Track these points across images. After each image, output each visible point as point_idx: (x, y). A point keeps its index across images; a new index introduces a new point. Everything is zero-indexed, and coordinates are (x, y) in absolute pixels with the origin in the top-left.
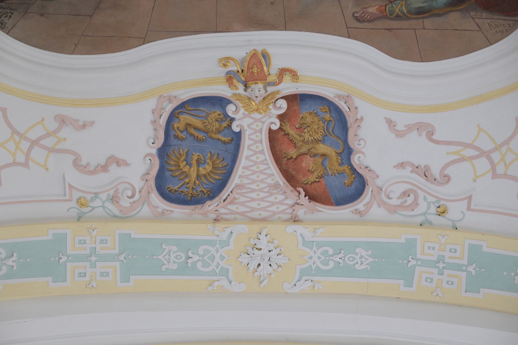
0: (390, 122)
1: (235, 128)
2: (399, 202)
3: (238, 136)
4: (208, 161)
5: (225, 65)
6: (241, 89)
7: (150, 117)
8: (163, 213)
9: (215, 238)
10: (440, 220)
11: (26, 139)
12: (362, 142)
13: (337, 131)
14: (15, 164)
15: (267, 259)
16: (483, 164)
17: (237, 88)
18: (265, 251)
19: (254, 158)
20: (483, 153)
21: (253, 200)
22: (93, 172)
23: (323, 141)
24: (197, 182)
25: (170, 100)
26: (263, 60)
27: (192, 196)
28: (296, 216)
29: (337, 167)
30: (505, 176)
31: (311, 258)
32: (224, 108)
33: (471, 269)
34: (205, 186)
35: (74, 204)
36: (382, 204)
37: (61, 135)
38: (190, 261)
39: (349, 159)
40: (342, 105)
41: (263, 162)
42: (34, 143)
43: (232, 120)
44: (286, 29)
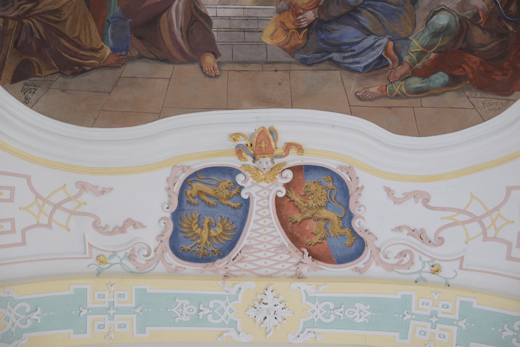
0: (389, 191)
1: (244, 195)
2: (396, 261)
3: (247, 202)
4: (219, 224)
5: (235, 140)
6: (249, 161)
7: (164, 184)
9: (224, 293)
10: (434, 278)
11: (49, 203)
12: (362, 209)
13: (339, 199)
14: (39, 225)
15: (272, 313)
16: (474, 228)
18: (271, 305)
19: (261, 222)
21: (260, 259)
22: (112, 233)
23: (326, 207)
24: (209, 243)
25: (183, 170)
26: (270, 136)
27: (204, 255)
28: (300, 274)
29: (338, 229)
30: (495, 239)
31: (313, 311)
32: (234, 177)
33: (462, 324)
34: (216, 246)
35: (93, 261)
36: (380, 262)
38: (201, 314)
39: (350, 223)
41: (269, 226)
42: (57, 206)
43: (241, 188)
44: (292, 108)
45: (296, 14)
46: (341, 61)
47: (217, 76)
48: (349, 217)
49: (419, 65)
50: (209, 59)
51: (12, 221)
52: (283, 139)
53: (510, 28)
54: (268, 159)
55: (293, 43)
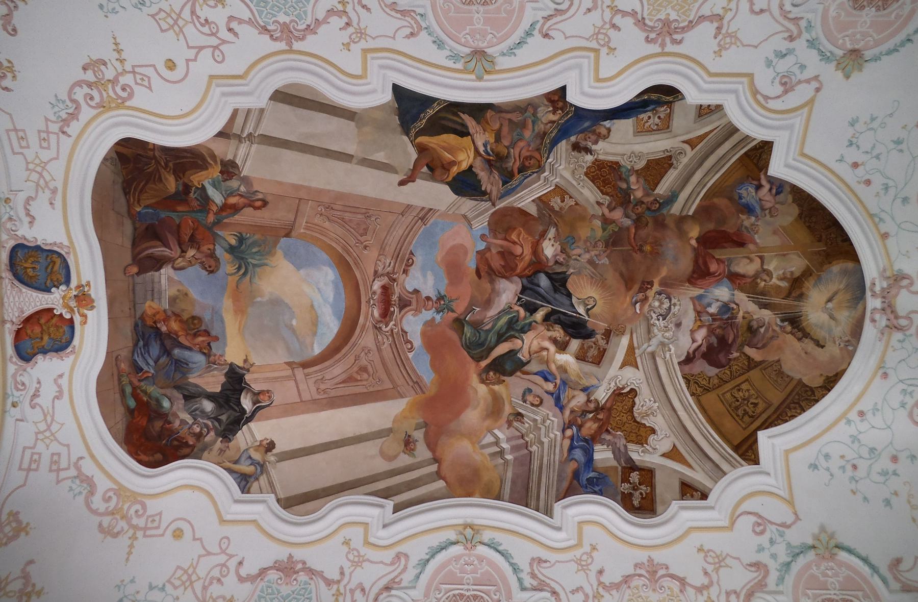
0: (61, 376)
1: (53, 290)
8: (4, 247)
11: (42, 170)
13: (56, 346)
14: (28, 163)
20: (49, 427)
21: (14, 298)
23: (50, 338)
30: (37, 439)
36: (17, 371)
37: (47, 191)
40: (69, 349)
42: (41, 174)
43: (58, 288)
48: (45, 352)
49: (139, 391)
50: (135, 270)
51: (28, 147)
52: (89, 314)
54: (75, 305)
55: (147, 319)
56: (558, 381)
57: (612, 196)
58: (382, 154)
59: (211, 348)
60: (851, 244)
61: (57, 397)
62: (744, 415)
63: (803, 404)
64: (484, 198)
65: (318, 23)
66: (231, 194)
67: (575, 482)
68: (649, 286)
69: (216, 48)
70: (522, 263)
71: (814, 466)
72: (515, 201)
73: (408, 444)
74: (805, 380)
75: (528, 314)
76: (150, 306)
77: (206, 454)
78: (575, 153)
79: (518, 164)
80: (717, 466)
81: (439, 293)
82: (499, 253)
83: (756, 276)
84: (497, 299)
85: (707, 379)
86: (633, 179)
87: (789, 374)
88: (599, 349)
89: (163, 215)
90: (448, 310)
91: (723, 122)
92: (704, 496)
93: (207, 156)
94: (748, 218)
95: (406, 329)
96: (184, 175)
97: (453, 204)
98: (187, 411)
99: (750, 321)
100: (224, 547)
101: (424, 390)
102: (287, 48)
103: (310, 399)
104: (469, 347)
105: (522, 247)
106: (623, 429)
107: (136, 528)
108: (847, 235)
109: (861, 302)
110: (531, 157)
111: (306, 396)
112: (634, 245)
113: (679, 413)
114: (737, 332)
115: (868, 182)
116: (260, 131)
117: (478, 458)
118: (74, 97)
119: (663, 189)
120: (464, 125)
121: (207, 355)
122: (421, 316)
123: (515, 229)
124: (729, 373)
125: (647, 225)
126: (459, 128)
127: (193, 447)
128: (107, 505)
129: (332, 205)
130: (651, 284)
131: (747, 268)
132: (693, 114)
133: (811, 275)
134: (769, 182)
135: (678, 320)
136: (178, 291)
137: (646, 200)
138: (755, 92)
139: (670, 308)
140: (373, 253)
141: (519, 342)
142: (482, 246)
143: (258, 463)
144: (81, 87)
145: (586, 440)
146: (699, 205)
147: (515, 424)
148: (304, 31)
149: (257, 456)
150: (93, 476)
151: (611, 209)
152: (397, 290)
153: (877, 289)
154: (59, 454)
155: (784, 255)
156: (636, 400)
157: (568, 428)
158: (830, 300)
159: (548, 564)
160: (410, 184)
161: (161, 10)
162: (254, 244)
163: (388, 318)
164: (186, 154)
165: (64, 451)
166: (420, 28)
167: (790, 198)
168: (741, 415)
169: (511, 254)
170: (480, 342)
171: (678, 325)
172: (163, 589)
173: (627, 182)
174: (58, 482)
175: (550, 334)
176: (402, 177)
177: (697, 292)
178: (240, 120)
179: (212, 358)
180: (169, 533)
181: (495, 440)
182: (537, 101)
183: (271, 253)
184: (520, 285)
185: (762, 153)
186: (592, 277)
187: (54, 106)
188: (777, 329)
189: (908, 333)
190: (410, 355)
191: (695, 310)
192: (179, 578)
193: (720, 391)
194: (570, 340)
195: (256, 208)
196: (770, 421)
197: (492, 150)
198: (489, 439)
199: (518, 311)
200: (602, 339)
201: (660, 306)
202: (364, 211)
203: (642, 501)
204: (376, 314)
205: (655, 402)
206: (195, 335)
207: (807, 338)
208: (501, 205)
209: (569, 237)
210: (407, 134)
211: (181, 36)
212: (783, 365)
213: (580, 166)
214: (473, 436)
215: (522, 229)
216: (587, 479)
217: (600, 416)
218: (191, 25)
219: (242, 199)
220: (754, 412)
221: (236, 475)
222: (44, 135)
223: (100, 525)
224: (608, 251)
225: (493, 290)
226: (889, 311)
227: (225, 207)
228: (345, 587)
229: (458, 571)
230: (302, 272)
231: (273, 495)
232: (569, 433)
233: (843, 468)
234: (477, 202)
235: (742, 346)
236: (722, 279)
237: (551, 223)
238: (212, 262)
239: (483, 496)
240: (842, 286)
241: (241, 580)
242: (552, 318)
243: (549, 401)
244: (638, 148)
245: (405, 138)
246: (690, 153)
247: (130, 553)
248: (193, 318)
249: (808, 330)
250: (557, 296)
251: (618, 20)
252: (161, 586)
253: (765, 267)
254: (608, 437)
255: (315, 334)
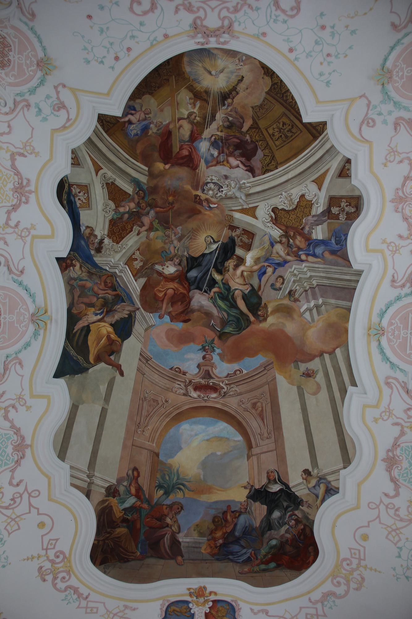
0: (252, 610)
1: (192, 612)
5: (189, 590)
6: (195, 598)
7: (159, 607)
11: (112, 613)
12: (241, 617)
17: (193, 598)
25: (168, 601)
26: (204, 589)
32: (188, 605)
40: (233, 604)
42: (115, 615)
43: (191, 609)
44: (213, 577)
45: (215, 541)
46: (233, 559)
47: (182, 565)
49: (264, 560)
50: (179, 558)
52: (209, 590)
53: (301, 545)
54: (203, 598)
56: (266, 264)
57: (133, 224)
58: (101, 387)
59: (235, 511)
60: (171, 58)
61: (267, 613)
62: (291, 132)
63: (284, 91)
64: (133, 315)
65: (13, 426)
66: (129, 492)
67: (338, 253)
68: (198, 198)
69: (30, 495)
70: (180, 289)
71: (328, 83)
72: (136, 294)
73: (309, 374)
74: (266, 90)
75: (217, 285)
76: (204, 550)
77: (310, 517)
78: (103, 251)
79: (109, 291)
80: (327, 151)
81: (201, 349)
82: (172, 306)
83: (192, 123)
84: (205, 308)
85: (265, 157)
86: (122, 210)
87: (262, 100)
88: (243, 234)
89: (142, 537)
90: (213, 343)
91: (83, 149)
92: (349, 161)
93: (103, 506)
94: (151, 129)
95: (225, 374)
96: (115, 522)
97: (137, 338)
98: (279, 529)
99: (224, 127)
100: (374, 506)
101: (270, 362)
102: (29, 448)
103: (274, 443)
104: (239, 329)
105: (169, 289)
106: (301, 218)
107: (359, 564)
108: (165, 62)
109: (212, 51)
110: (105, 282)
111: (272, 446)
112: (168, 208)
113: (290, 177)
114: (232, 136)
115: (129, 49)
116: (85, 469)
117: (320, 324)
118: (63, 588)
119: (129, 188)
120: (82, 329)
121: (240, 513)
122: (216, 363)
123: (155, 294)
124: (261, 142)
125: (154, 199)
126: (84, 333)
127: (305, 526)
128: (342, 585)
129: (137, 423)
130: (196, 196)
131: (186, 129)
132: (77, 169)
133: (192, 86)
134: (126, 116)
135: (222, 177)
136: (194, 530)
137: (137, 200)
138: (64, 127)
139: (214, 183)
140: (171, 396)
141: (237, 292)
142: (167, 318)
143: (319, 481)
144: (56, 584)
145: (309, 245)
146: (141, 163)
147: (297, 296)
148: (18, 436)
149: (313, 482)
150: (322, 593)
151: (142, 225)
152: (198, 380)
153: (202, 40)
154: (307, 614)
155: (178, 104)
156: (280, 208)
157: (300, 257)
158: (210, 73)
159: (395, 275)
160: (123, 368)
161: (5, 528)
162: (163, 478)
163: (218, 387)
164: (102, 520)
165: (304, 611)
166: (17, 358)
167: (138, 101)
168: (291, 134)
169: (173, 297)
170: (236, 321)
171: (226, 177)
172: (400, 549)
173: (124, 213)
174: (325, 615)
175: (231, 270)
176: (117, 374)
177: (203, 164)
178: (78, 483)
179: (242, 510)
180: (363, 543)
181: (308, 311)
182: (66, 278)
183: (170, 467)
184: (196, 290)
185: (106, 121)
186: (191, 238)
187: (70, 603)
188: (230, 108)
189: (234, 19)
190: (245, 372)
191: (215, 165)
192: (394, 537)
193: (274, 148)
194: (236, 255)
195: (139, 475)
196: (295, 114)
197: (99, 310)
198: (307, 315)
199: (214, 293)
200: (235, 231)
201: (213, 190)
202: (141, 402)
203: (352, 205)
204: (214, 395)
205: (282, 194)
206: (226, 521)
207: (236, 88)
208: (138, 303)
209: (162, 256)
210: (88, 369)
211: (23, 517)
212: (256, 105)
213: (112, 247)
214: (304, 328)
215: (156, 289)
216: (337, 244)
217: (292, 234)
218: (16, 510)
219: (133, 484)
220: (289, 125)
221: (326, 497)
222: (89, 610)
223: (357, 589)
224: (172, 227)
225: (199, 310)
226: (218, 33)
227: (138, 496)
228: (405, 422)
229: (398, 341)
230: (183, 446)
231: (341, 471)
232: (303, 257)
233: (329, 63)
234: (136, 319)
235: (241, 133)
236: (194, 147)
237: (152, 268)
238: (175, 507)
239: (348, 321)
240: (200, 65)
241: (397, 494)
242: (220, 268)
243: (280, 271)
244: (100, 207)
245: (90, 370)
246: (105, 170)
247: (376, 570)
248: (214, 521)
249: (231, 88)
250: (204, 263)
251: (12, 223)
252: (399, 550)
253: (186, 117)
254: (307, 229)
255: (228, 439)
